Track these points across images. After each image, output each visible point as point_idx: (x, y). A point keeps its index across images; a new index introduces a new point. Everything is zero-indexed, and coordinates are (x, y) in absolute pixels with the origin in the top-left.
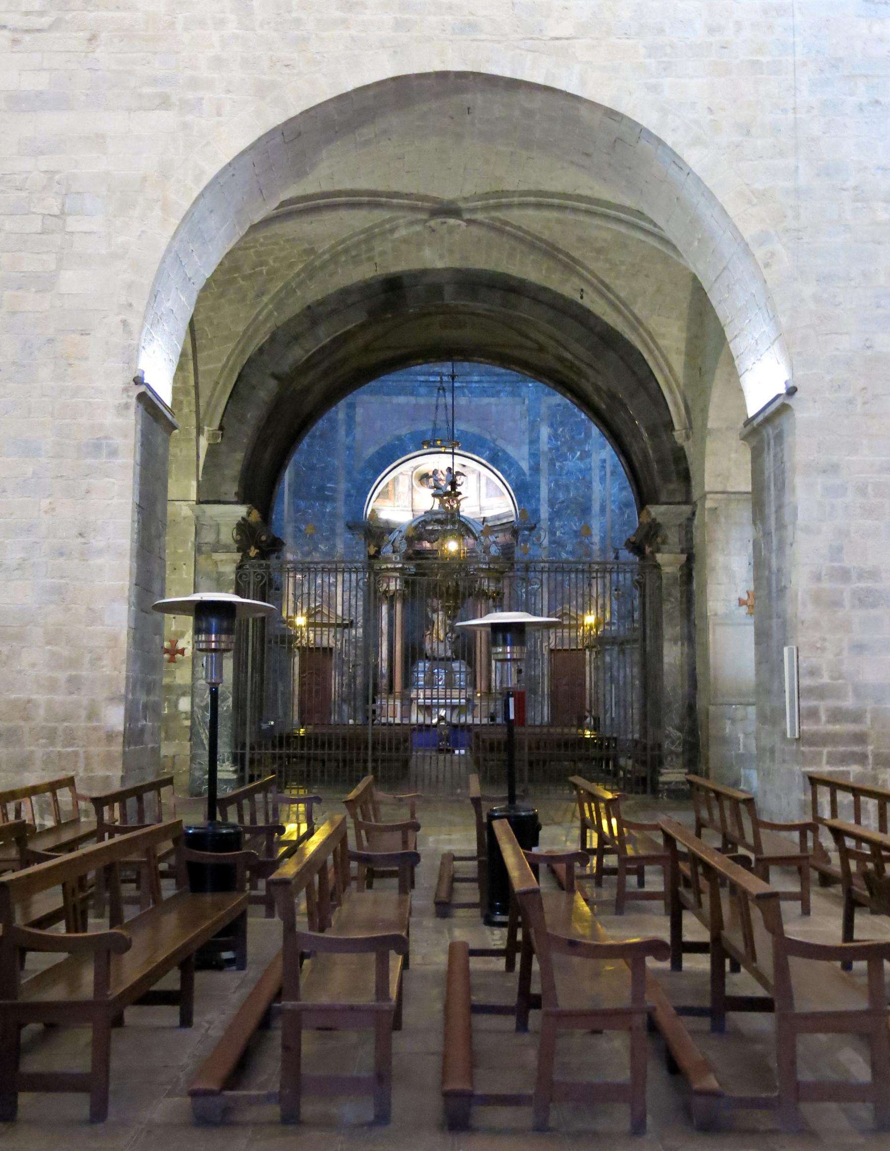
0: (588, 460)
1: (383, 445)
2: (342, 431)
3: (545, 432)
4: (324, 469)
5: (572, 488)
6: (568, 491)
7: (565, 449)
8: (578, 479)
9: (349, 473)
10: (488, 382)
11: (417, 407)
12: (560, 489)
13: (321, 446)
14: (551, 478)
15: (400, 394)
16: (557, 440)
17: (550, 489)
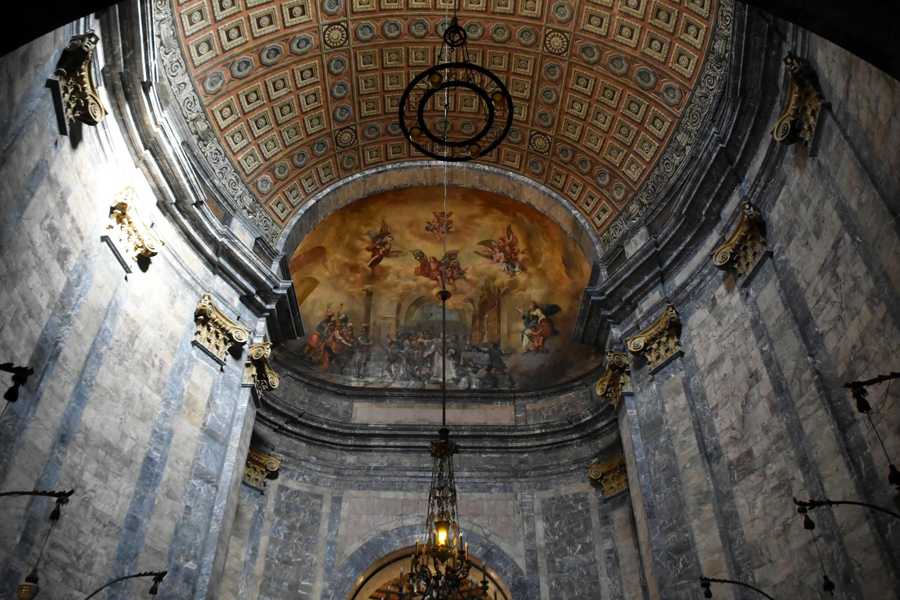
0: (591, 553)
1: (369, 538)
2: (324, 525)
3: (540, 527)
4: (300, 563)
5: (576, 585)
6: (572, 588)
7: (564, 543)
8: (582, 575)
9: (328, 570)
10: (479, 478)
11: (405, 502)
12: (562, 588)
13: (300, 539)
14: (551, 575)
15: (388, 489)
16: (554, 535)
17: (551, 589)
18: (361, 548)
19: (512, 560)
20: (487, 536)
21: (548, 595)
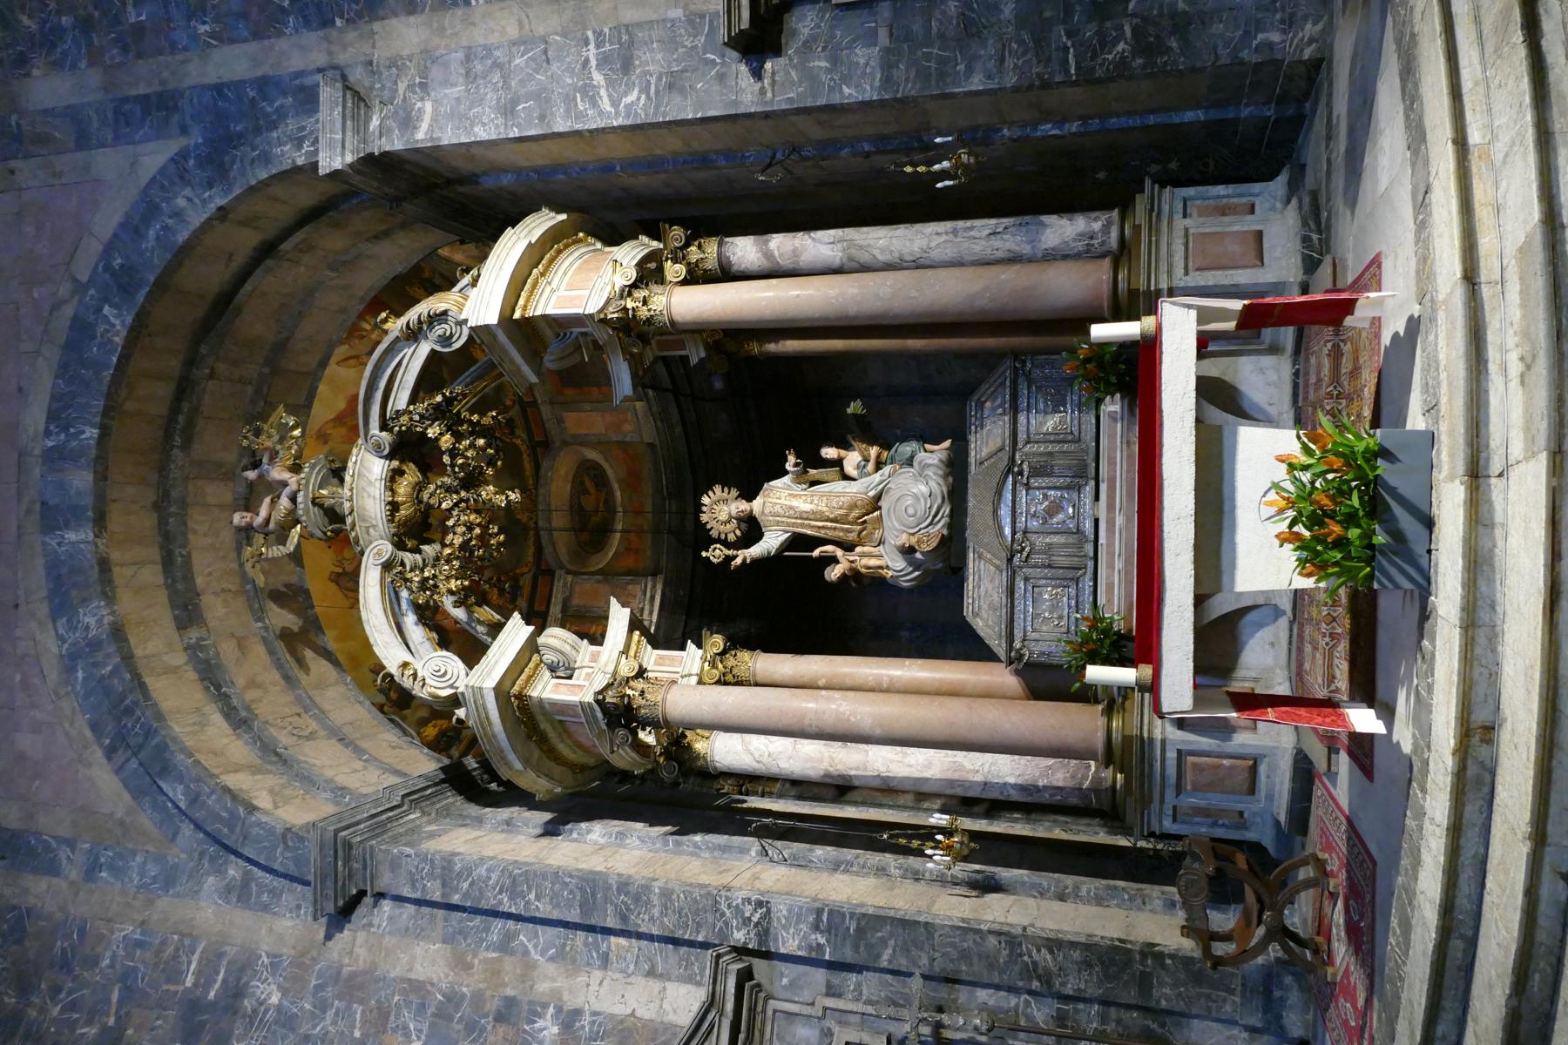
9: (168, 880)
18: (110, 753)
19: (145, 191)
20: (79, 288)
21: (238, 49)
